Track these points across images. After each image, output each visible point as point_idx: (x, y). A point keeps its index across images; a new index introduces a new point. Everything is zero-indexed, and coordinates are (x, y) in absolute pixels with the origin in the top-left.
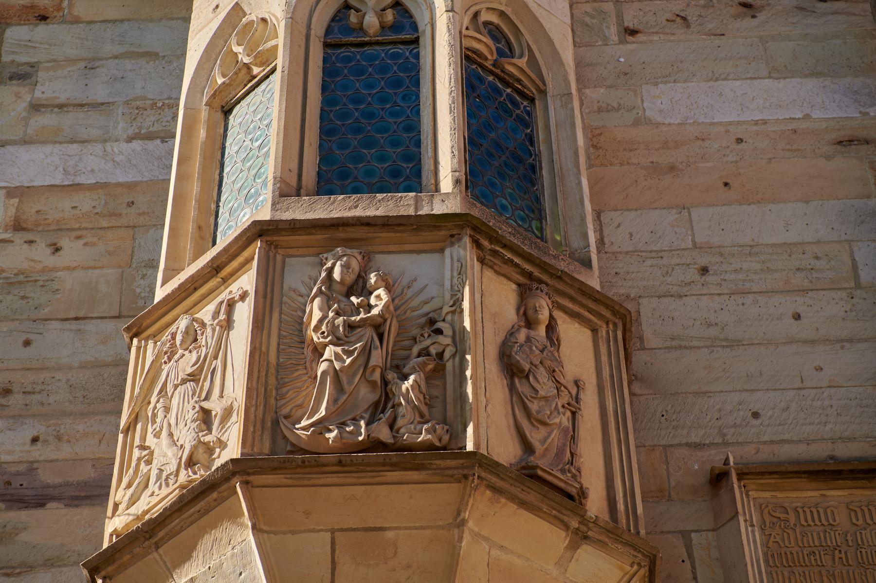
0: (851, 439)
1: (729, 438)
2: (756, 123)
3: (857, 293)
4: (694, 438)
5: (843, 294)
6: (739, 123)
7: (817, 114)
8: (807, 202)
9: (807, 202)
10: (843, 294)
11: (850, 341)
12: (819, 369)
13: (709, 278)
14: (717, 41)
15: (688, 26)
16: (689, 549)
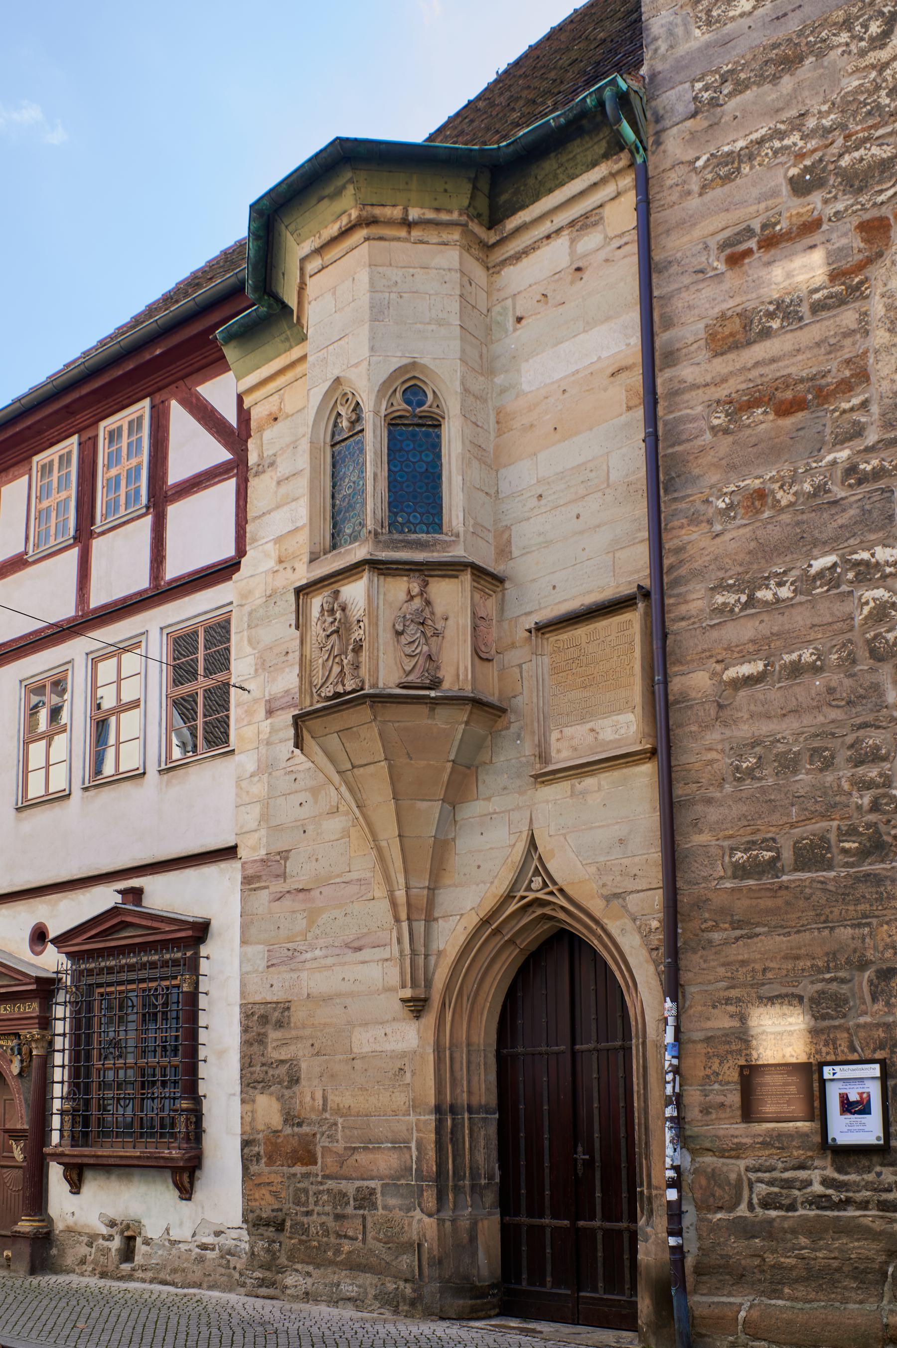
0: (590, 592)
1: (542, 605)
2: (573, 374)
3: (607, 491)
4: (528, 610)
5: (600, 494)
6: (565, 377)
7: (605, 354)
8: (591, 429)
9: (591, 429)
10: (600, 494)
11: (599, 526)
12: (584, 549)
13: (543, 502)
14: (561, 309)
15: (547, 303)
16: (521, 673)
